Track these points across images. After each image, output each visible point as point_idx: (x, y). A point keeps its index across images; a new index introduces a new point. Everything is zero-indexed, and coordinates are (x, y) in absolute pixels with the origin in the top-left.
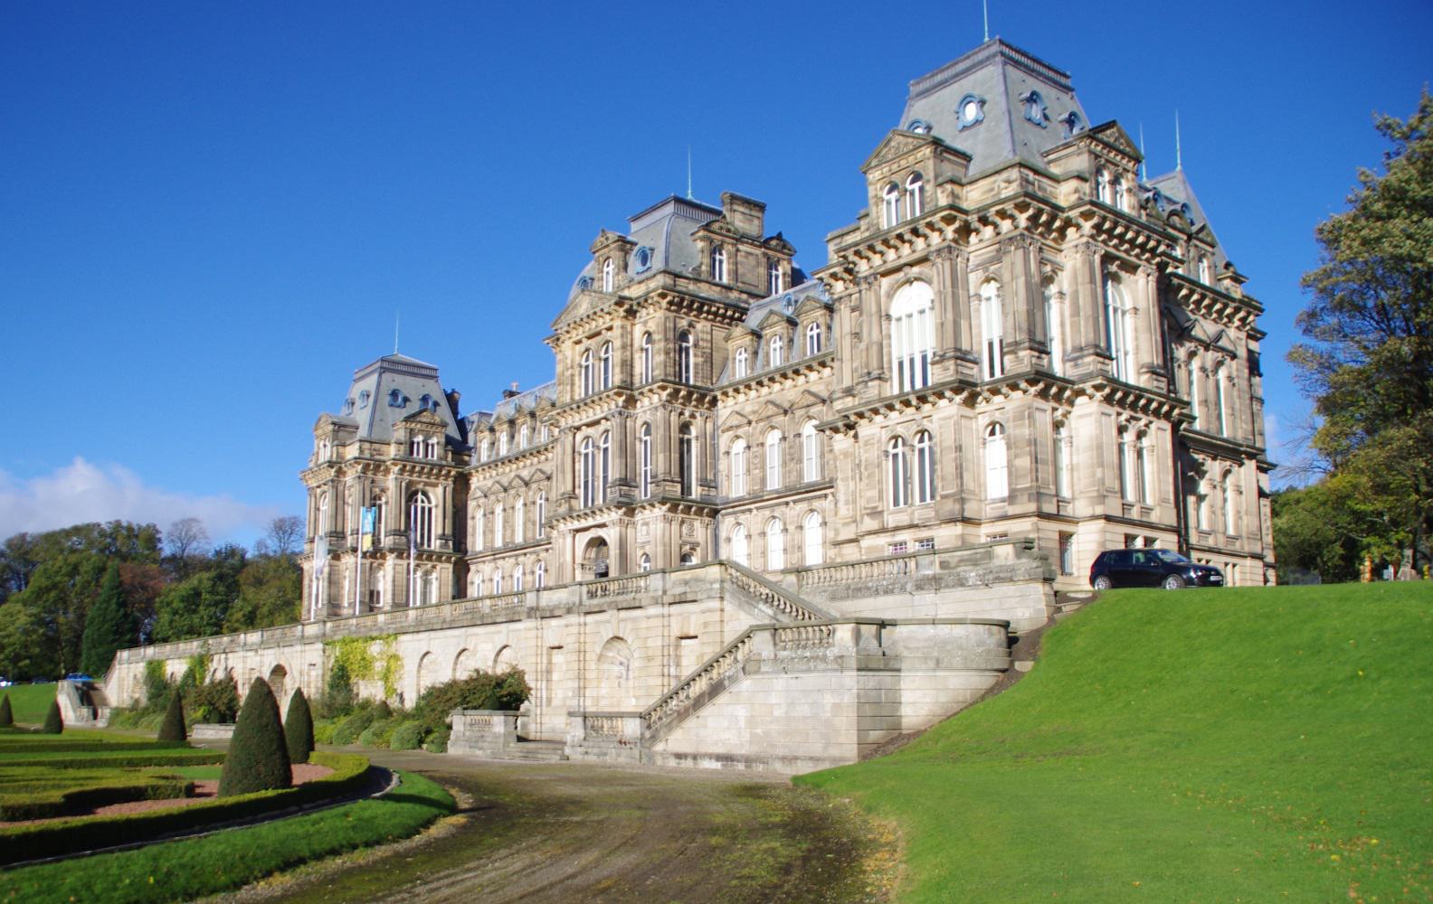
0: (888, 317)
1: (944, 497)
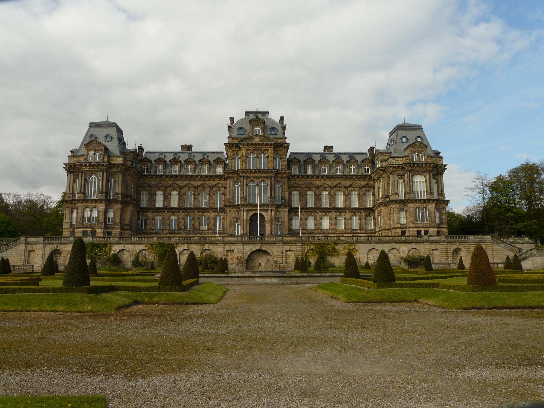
0: (413, 181)
1: (432, 222)
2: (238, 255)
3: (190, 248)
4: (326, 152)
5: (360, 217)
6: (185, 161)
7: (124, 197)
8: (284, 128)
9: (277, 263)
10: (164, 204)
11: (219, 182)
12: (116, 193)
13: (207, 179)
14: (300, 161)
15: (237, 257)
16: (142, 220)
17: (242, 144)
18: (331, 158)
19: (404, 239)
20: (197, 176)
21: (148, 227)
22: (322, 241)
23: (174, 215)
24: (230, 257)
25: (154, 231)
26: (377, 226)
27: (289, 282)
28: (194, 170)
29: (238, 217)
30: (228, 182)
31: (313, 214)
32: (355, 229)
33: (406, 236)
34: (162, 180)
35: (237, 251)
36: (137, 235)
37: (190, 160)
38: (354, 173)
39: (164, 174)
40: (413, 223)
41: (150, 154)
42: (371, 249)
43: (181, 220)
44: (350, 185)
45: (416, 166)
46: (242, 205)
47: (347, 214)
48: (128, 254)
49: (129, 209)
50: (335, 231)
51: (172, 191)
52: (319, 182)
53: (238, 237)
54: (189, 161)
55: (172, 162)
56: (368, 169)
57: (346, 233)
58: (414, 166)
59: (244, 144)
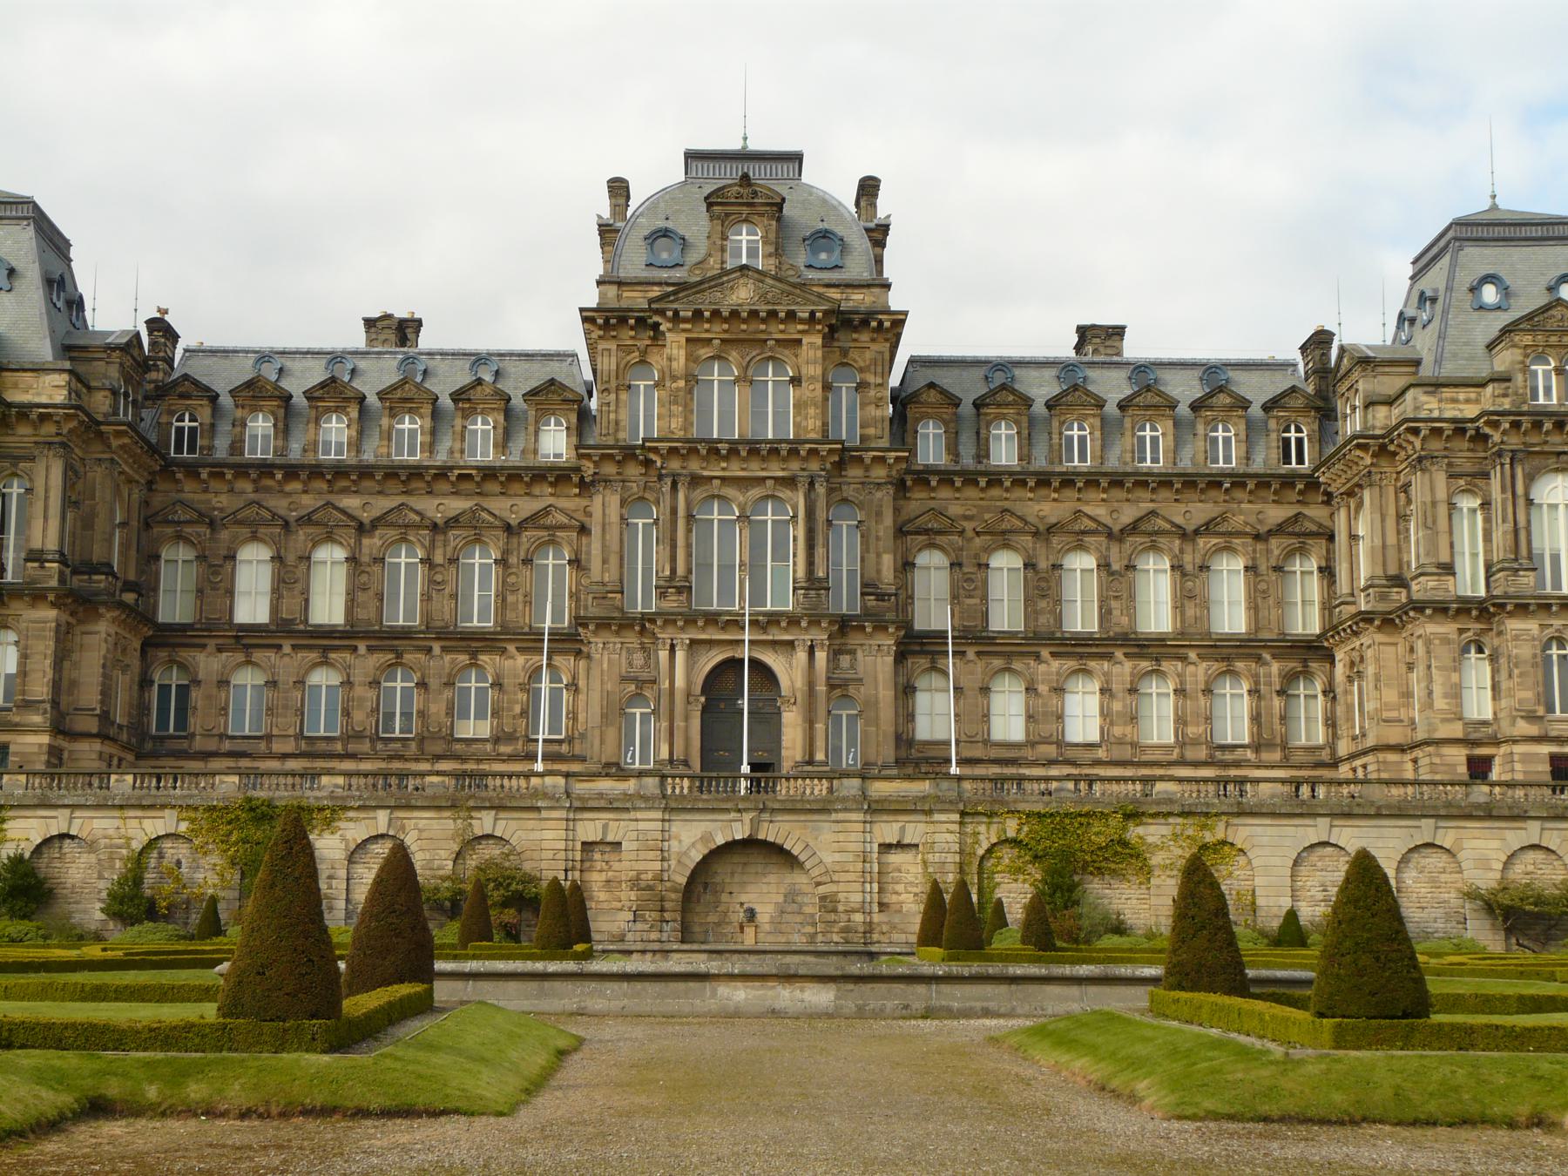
0: (1530, 502)
2: (641, 866)
3: (403, 828)
4: (1089, 358)
5: (1257, 683)
6: (382, 395)
7: (75, 572)
8: (879, 235)
9: (835, 911)
10: (275, 609)
11: (551, 500)
12: (31, 551)
13: (493, 487)
14: (955, 402)
15: (638, 879)
16: (165, 689)
17: (670, 314)
18: (1113, 387)
19: (1482, 799)
20: (442, 473)
21: (195, 723)
22: (1061, 801)
23: (325, 663)
24: (603, 876)
25: (227, 746)
26: (1343, 730)
27: (890, 1005)
28: (428, 439)
29: (645, 676)
30: (598, 499)
31: (1017, 665)
32: (1229, 741)
33: (1492, 785)
34: (268, 490)
35: (635, 845)
36: (142, 763)
37: (409, 391)
38: (1227, 459)
39: (279, 461)
40: (1531, 717)
41: (209, 361)
42: (1312, 846)
43: (359, 691)
44: (1207, 524)
45: (1548, 426)
46: (669, 619)
47: (1191, 668)
48: (88, 859)
49: (101, 632)
50: (1126, 753)
51: (316, 544)
52: (1048, 508)
53: (641, 774)
54: (400, 398)
55: (321, 399)
56: (1300, 442)
57: (1182, 762)
58: (1537, 425)
59: (676, 313)
